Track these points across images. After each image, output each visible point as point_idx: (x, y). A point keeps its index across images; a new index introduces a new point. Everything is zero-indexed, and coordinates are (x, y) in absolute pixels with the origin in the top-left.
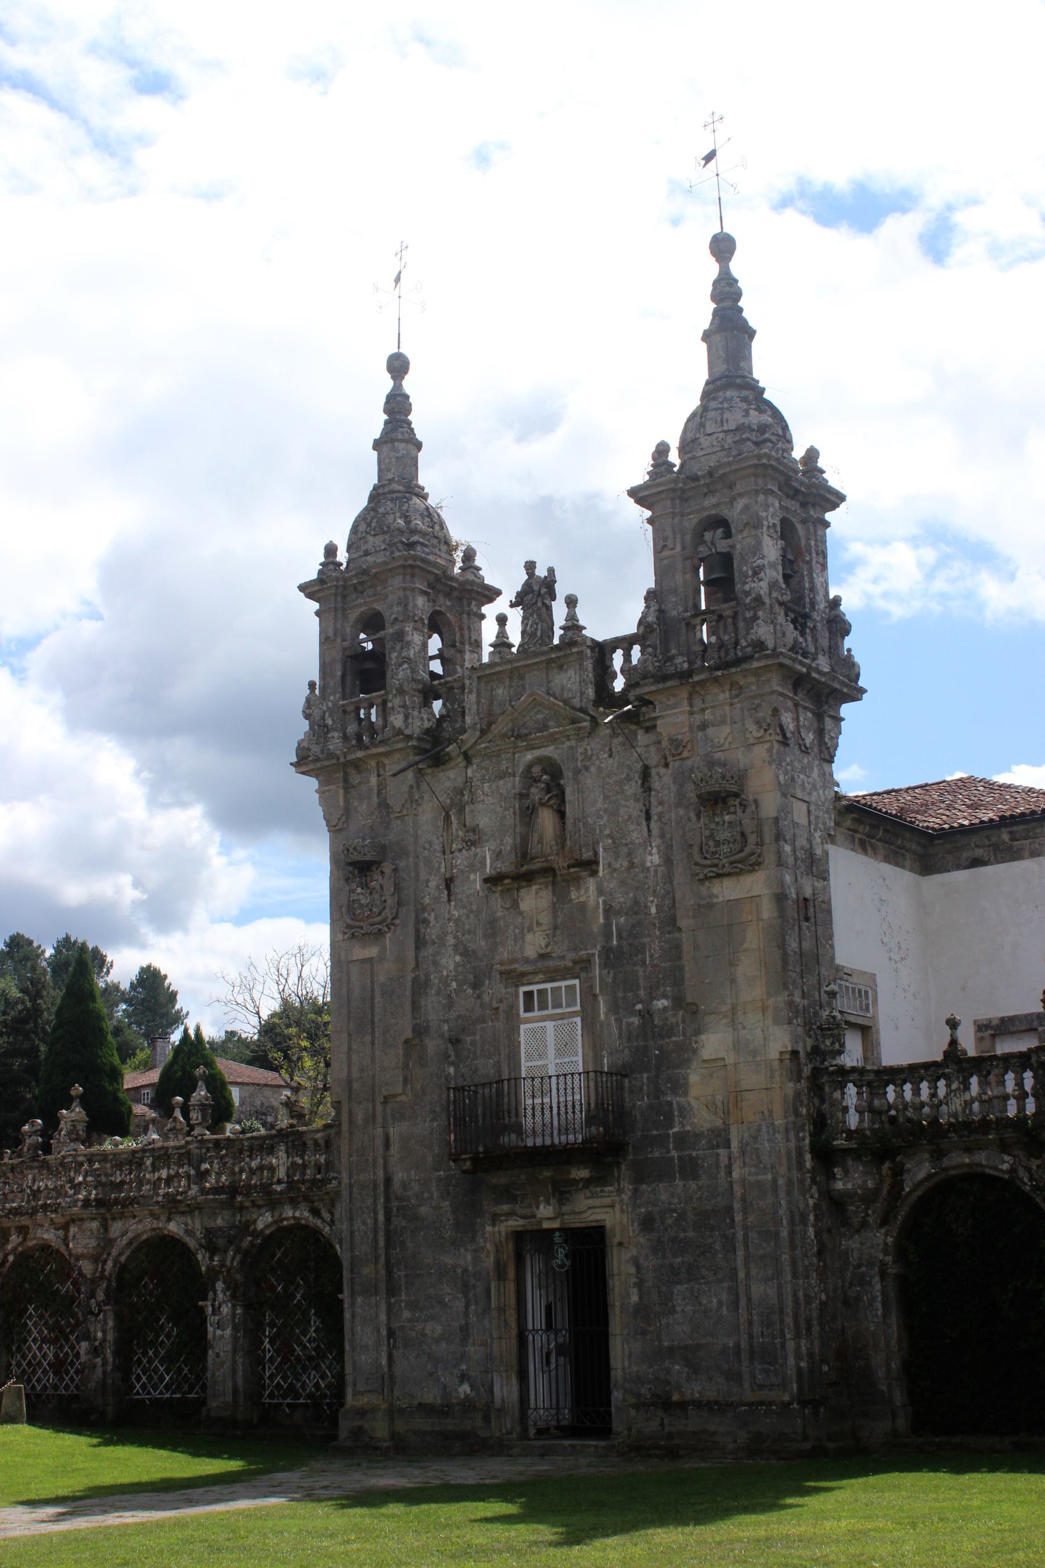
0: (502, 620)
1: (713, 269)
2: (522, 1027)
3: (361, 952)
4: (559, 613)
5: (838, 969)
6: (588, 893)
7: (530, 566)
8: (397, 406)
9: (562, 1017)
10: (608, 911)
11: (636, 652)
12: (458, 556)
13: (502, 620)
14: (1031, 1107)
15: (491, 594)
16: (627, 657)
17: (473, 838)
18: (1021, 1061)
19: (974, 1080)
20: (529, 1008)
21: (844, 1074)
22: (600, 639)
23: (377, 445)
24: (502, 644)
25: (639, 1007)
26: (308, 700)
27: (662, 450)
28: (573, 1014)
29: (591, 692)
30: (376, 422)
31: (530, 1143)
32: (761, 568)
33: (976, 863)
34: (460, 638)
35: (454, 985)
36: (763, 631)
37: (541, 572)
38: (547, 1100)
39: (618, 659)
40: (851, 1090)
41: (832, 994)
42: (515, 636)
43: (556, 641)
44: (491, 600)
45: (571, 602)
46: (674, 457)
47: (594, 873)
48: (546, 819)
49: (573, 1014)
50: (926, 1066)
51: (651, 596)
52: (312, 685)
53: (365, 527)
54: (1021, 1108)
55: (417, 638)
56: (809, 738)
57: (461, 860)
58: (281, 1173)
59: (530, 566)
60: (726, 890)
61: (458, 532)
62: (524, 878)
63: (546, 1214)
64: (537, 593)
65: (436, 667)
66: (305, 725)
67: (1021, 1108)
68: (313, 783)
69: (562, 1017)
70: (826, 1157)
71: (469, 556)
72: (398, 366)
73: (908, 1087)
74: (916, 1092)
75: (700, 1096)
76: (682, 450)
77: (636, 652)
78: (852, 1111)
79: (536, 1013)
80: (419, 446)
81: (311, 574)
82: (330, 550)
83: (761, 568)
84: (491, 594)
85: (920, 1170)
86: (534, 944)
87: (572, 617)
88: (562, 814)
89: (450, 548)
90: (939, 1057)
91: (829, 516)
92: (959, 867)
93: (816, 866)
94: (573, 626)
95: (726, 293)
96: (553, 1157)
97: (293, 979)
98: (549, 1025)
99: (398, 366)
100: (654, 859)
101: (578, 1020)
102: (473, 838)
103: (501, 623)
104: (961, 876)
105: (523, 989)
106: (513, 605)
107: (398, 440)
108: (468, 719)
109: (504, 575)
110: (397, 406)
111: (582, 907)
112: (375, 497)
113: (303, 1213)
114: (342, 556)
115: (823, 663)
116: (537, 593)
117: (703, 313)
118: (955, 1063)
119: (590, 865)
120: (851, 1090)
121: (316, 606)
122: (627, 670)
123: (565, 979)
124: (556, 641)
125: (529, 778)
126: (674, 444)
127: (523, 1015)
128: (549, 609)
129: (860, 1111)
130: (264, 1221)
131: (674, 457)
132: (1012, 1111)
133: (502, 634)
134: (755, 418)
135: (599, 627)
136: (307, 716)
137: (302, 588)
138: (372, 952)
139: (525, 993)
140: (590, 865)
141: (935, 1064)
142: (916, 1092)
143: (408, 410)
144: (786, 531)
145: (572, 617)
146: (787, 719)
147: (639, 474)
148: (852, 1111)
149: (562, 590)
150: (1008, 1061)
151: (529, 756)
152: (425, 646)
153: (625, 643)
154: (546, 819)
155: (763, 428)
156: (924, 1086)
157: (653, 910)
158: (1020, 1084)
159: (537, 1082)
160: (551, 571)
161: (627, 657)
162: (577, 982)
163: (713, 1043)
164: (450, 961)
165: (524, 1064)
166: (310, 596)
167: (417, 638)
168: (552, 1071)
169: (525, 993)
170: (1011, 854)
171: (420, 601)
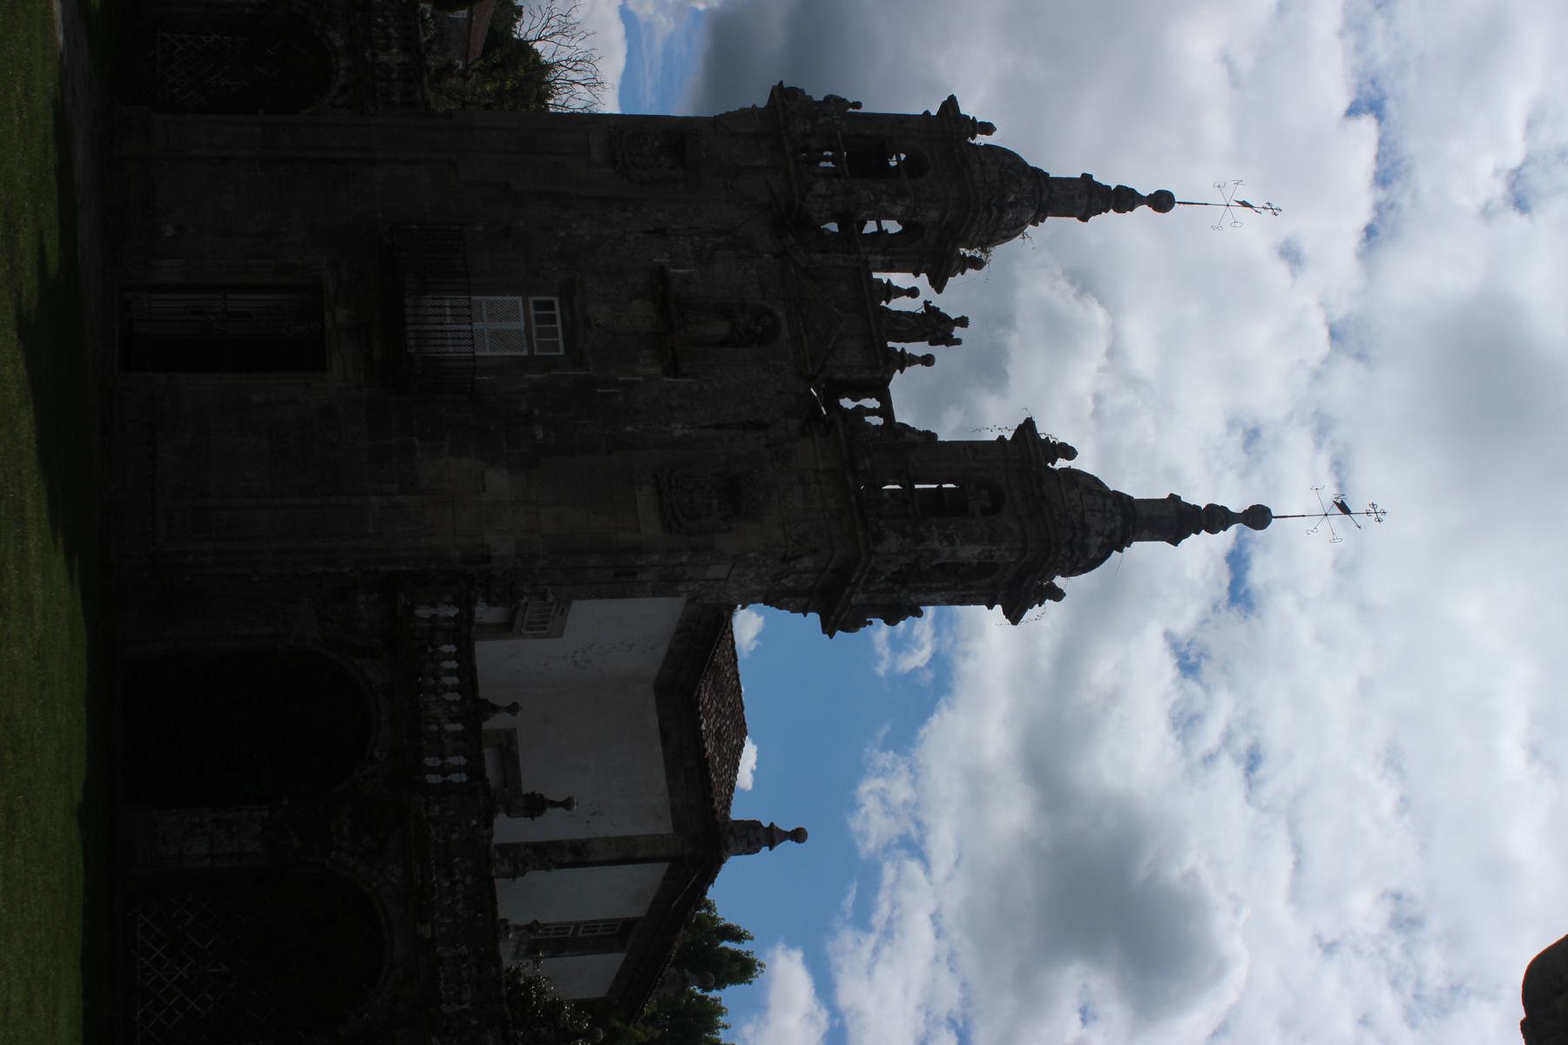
0: (913, 292)
1: (1236, 507)
2: (519, 299)
4: (917, 348)
5: (568, 604)
7: (963, 322)
8: (1124, 199)
9: (529, 337)
11: (876, 421)
12: (976, 253)
13: (913, 292)
14: (433, 779)
15: (938, 284)
16: (873, 412)
18: (476, 770)
19: (459, 727)
20: (538, 305)
21: (467, 605)
22: (891, 386)
23: (1087, 178)
24: (892, 291)
25: (537, 412)
26: (844, 101)
27: (1069, 452)
28: (531, 349)
29: (841, 375)
30: (1109, 178)
31: (407, 302)
32: (952, 543)
33: (665, 736)
34: (898, 254)
35: (562, 234)
36: (892, 543)
37: (957, 332)
38: (449, 320)
39: (872, 403)
40: (453, 612)
41: (544, 596)
42: (898, 304)
43: (890, 344)
44: (932, 283)
45: (928, 360)
46: (1061, 463)
47: (666, 373)
48: (719, 329)
49: (531, 349)
50: (474, 682)
51: (930, 436)
52: (858, 105)
53: (1007, 161)
54: (432, 770)
55: (898, 209)
56: (789, 583)
58: (383, 58)
59: (963, 322)
61: (998, 252)
64: (937, 327)
65: (870, 227)
66: (819, 97)
67: (432, 770)
68: (762, 102)
69: (529, 337)
71: (977, 264)
72: (1162, 201)
73: (454, 664)
74: (450, 673)
76: (1068, 471)
77: (876, 421)
78: (433, 611)
79: (532, 312)
80: (1084, 219)
81: (967, 108)
82: (988, 128)
83: (952, 543)
84: (938, 284)
87: (913, 360)
88: (723, 343)
89: (985, 245)
90: (482, 695)
91: (998, 608)
92: (662, 718)
93: (665, 585)
94: (905, 361)
97: (573, 76)
98: (521, 325)
99: (1162, 201)
100: (678, 430)
101: (525, 353)
103: (910, 292)
104: (653, 721)
105: (556, 300)
106: (926, 303)
107: (1090, 198)
108: (818, 256)
109: (956, 296)
110: (1124, 199)
112: (1038, 174)
114: (981, 140)
115: (859, 598)
116: (937, 327)
118: (476, 709)
119: (673, 369)
120: (453, 612)
121: (934, 113)
122: (861, 411)
123: (565, 341)
124: (890, 344)
126: (1073, 464)
127: (531, 299)
128: (921, 339)
129: (433, 618)
130: (337, 39)
131: (1061, 463)
132: (430, 761)
133: (899, 292)
134: (1095, 541)
135: (901, 385)
136: (828, 99)
137: (952, 99)
139: (552, 303)
141: (475, 690)
142: (450, 673)
143: (1119, 210)
144: (986, 568)
145: (913, 360)
146: (808, 562)
147: (1052, 428)
148: (433, 611)
149: (939, 351)
150: (479, 758)
151: (780, 314)
152: (891, 217)
153: (886, 410)
154: (719, 329)
155: (1085, 549)
156: (455, 680)
157: (629, 429)
158: (456, 769)
159: (466, 311)
160: (958, 342)
161: (873, 412)
162: (562, 352)
163: (499, 482)
165: (483, 300)
166: (944, 105)
167: (898, 209)
168: (476, 326)
169: (552, 303)
170: (673, 765)
171: (934, 214)
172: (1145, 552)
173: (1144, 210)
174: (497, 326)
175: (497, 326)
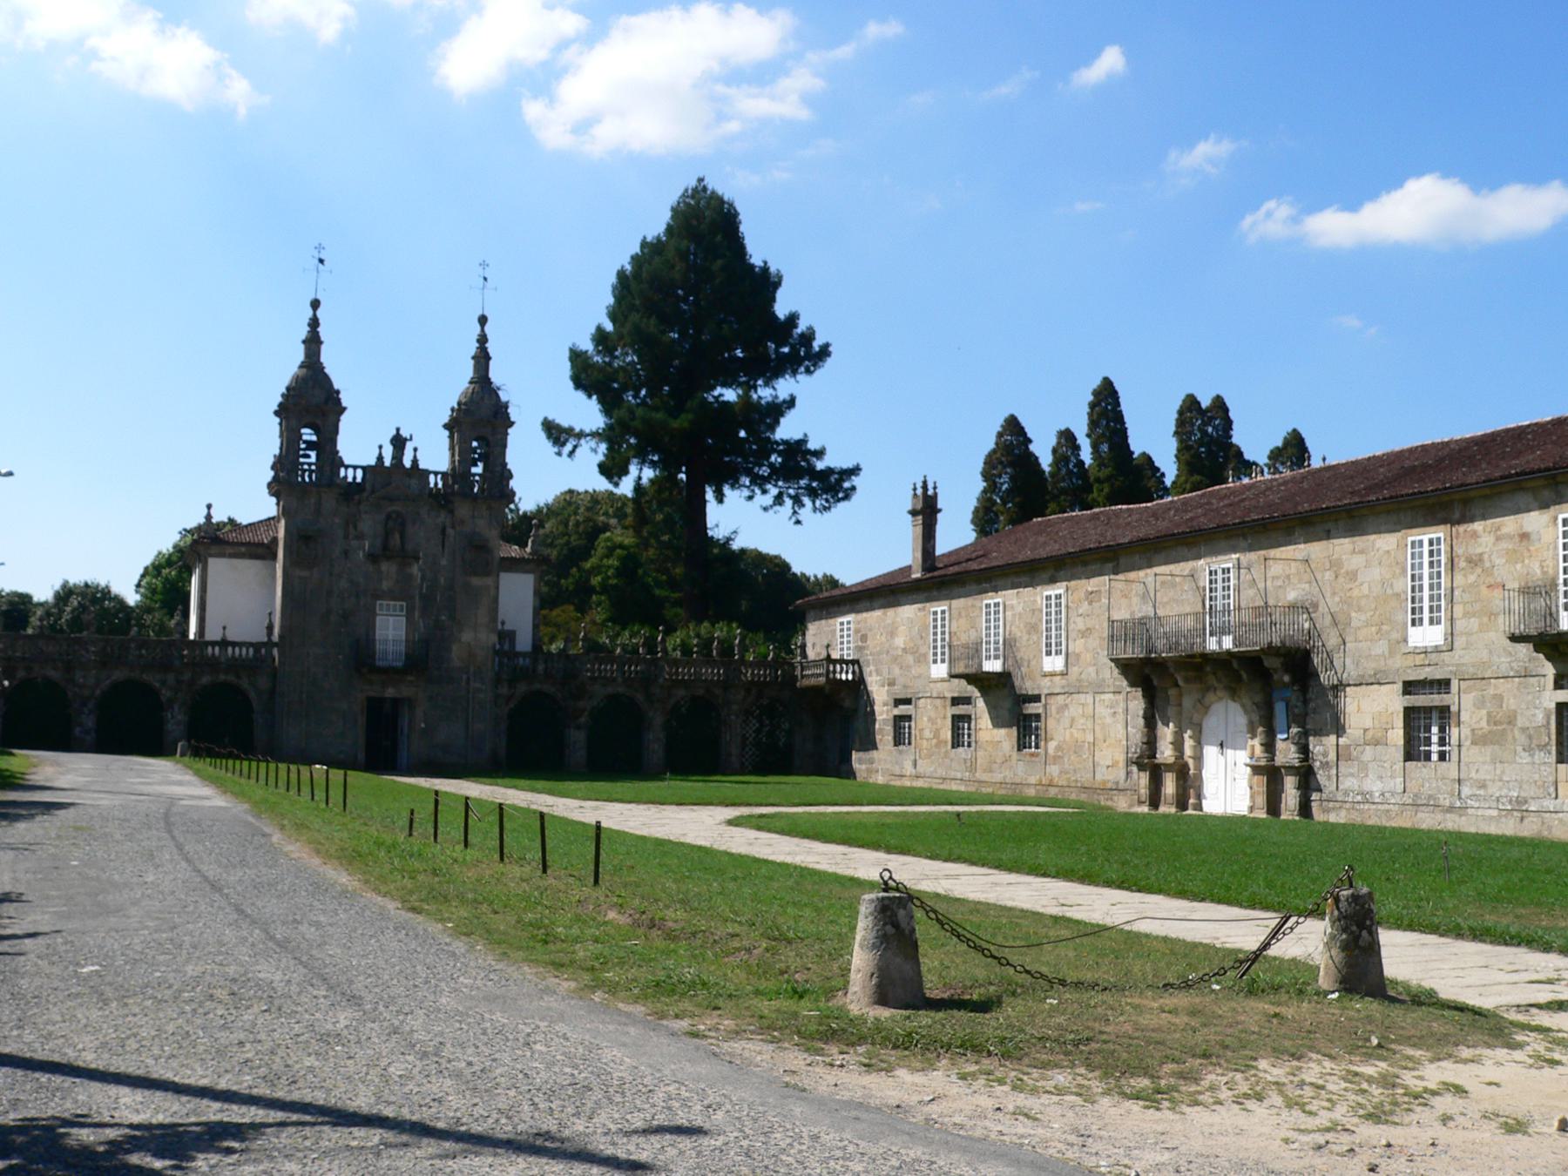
3: (299, 573)
6: (415, 570)
8: (314, 323)
10: (423, 578)
17: (361, 537)
24: (380, 458)
39: (432, 478)
45: (415, 450)
48: (397, 536)
57: (354, 543)
60: (476, 581)
62: (389, 558)
63: (390, 692)
70: (498, 681)
72: (315, 304)
75: (456, 654)
85: (522, 688)
86: (385, 585)
94: (415, 461)
95: (483, 340)
96: (388, 671)
99: (315, 304)
100: (444, 562)
102: (361, 537)
111: (410, 576)
113: (231, 678)
117: (473, 347)
125: (389, 517)
130: (205, 680)
138: (305, 573)
140: (417, 559)
153: (436, 474)
163: (467, 636)
164: (344, 584)
172: (496, 375)
173: (319, 313)
174: (391, 629)
175: (391, 629)
